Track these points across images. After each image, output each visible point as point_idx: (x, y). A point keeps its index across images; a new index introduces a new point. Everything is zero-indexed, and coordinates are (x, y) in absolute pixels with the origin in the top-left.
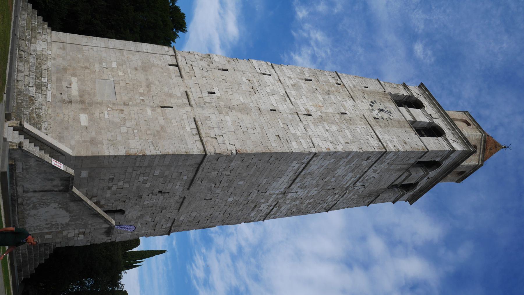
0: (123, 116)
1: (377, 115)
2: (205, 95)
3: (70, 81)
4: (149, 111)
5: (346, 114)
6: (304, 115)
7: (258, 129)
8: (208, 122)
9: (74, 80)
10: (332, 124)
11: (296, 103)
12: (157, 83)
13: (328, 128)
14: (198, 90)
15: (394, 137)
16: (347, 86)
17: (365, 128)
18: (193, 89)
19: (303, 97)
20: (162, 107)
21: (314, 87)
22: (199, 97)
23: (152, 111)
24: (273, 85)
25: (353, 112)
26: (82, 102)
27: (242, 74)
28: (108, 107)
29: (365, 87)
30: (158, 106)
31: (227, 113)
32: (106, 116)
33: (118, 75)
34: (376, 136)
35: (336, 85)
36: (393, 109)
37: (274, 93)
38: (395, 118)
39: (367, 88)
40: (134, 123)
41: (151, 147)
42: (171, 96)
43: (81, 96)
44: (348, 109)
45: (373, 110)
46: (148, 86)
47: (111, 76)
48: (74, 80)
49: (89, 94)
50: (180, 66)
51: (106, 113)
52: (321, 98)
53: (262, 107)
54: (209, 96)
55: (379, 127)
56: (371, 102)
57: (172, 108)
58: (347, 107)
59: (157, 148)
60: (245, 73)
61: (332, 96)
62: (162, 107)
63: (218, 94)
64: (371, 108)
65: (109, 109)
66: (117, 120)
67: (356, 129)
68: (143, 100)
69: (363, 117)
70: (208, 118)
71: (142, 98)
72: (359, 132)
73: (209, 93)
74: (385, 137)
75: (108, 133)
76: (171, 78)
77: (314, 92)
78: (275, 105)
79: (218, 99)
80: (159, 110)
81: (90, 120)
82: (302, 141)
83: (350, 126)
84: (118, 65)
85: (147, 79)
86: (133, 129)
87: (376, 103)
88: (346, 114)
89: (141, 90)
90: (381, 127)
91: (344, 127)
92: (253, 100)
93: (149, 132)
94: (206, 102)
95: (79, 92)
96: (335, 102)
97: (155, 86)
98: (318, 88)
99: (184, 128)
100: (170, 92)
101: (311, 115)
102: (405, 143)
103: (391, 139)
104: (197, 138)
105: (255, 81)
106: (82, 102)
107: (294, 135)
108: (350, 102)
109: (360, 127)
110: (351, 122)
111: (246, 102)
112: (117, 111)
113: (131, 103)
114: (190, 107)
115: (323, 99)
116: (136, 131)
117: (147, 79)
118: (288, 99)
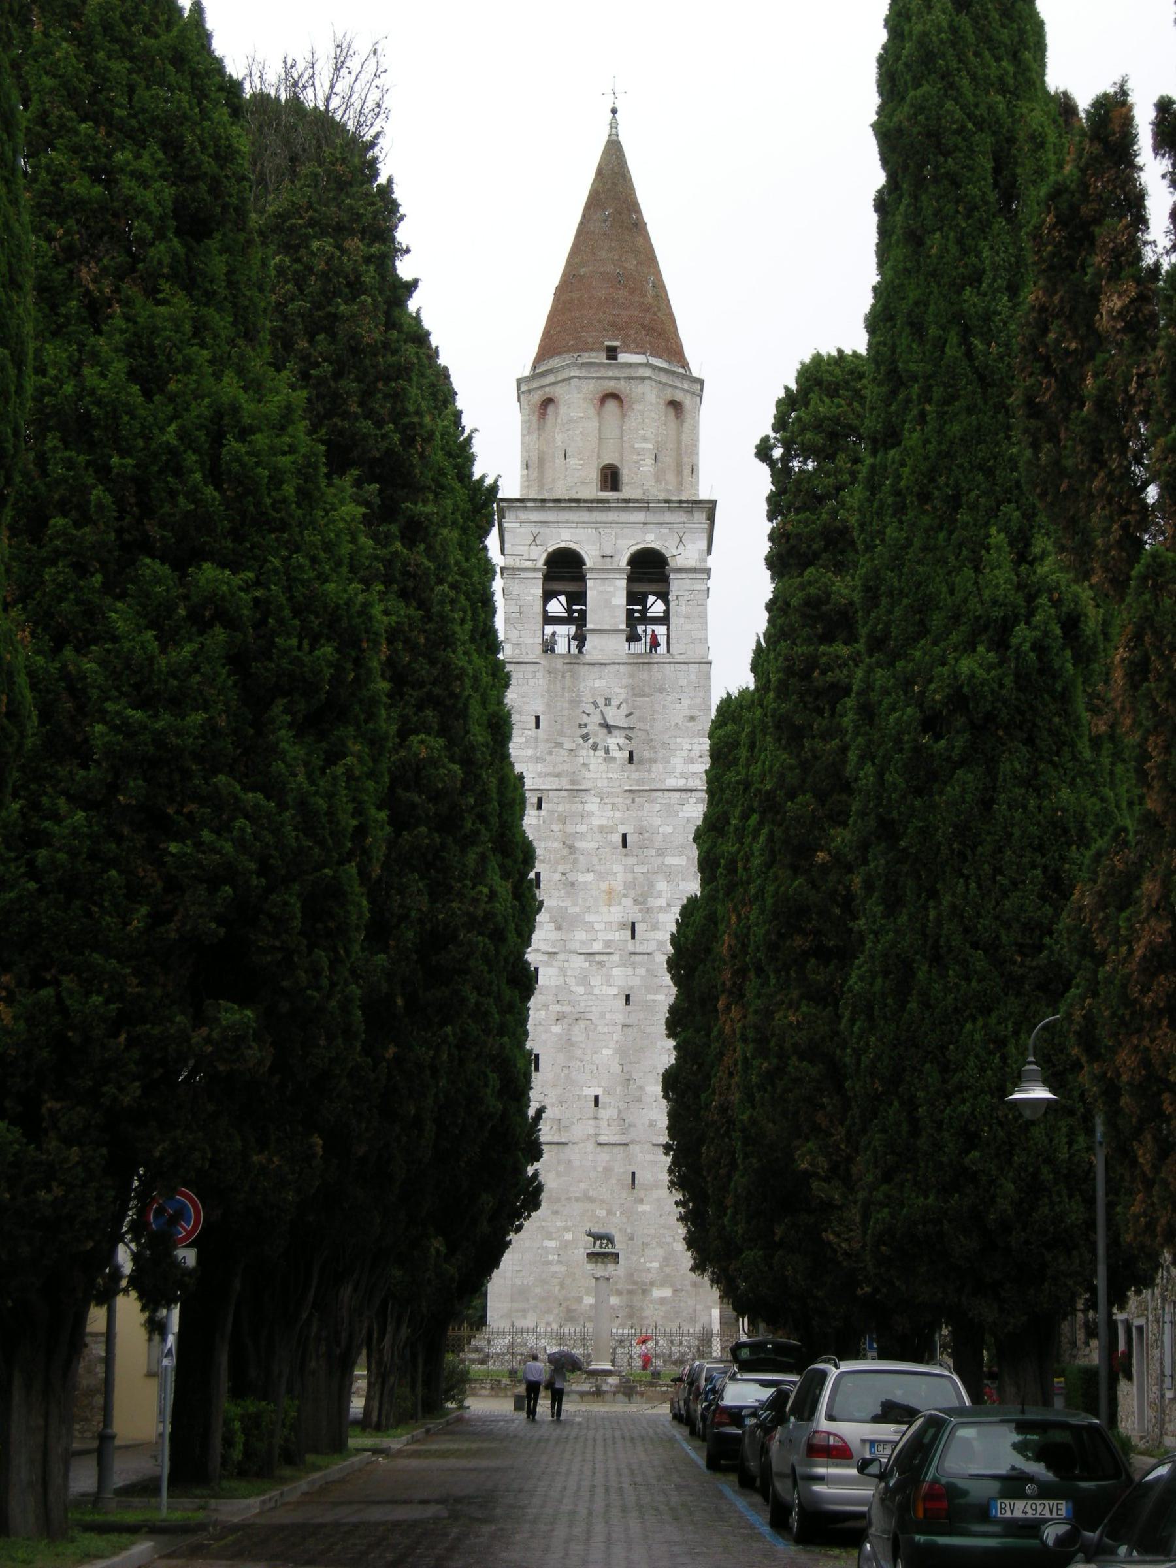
1: (620, 748)
2: (602, 1112)
4: (641, 1208)
5: (624, 836)
6: (633, 937)
10: (652, 886)
11: (608, 943)
12: (583, 1186)
13: (662, 902)
14: (591, 1122)
15: (679, 740)
16: (541, 780)
17: (658, 807)
18: (592, 1132)
19: (589, 918)
20: (633, 1188)
21: (557, 876)
24: (563, 971)
25: (618, 814)
26: (630, 1292)
27: (541, 1028)
29: (537, 727)
34: (677, 795)
35: (543, 813)
36: (597, 683)
37: (584, 980)
38: (623, 696)
39: (537, 718)
40: (666, 1232)
42: (608, 1170)
44: (611, 823)
45: (607, 750)
46: (591, 1200)
47: (576, 1251)
51: (648, 1265)
52: (589, 877)
53: (620, 1018)
54: (604, 1108)
55: (655, 767)
56: (585, 737)
58: (604, 822)
61: (578, 845)
63: (599, 1092)
64: (601, 753)
66: (660, 1252)
67: (664, 835)
69: (632, 795)
71: (618, 1214)
72: (669, 829)
74: (679, 769)
77: (573, 884)
78: (614, 991)
81: (662, 1285)
83: (656, 845)
84: (549, 1236)
85: (577, 1200)
87: (585, 725)
88: (624, 836)
89: (602, 1213)
90: (653, 761)
91: (660, 859)
92: (606, 1030)
96: (595, 845)
98: (561, 868)
100: (600, 1169)
101: (633, 924)
102: (692, 718)
103: (685, 753)
105: (558, 1008)
108: (592, 805)
109: (658, 821)
110: (647, 835)
111: (612, 1044)
113: (629, 1231)
114: (631, 1146)
115: (588, 871)
117: (577, 1200)
118: (598, 958)
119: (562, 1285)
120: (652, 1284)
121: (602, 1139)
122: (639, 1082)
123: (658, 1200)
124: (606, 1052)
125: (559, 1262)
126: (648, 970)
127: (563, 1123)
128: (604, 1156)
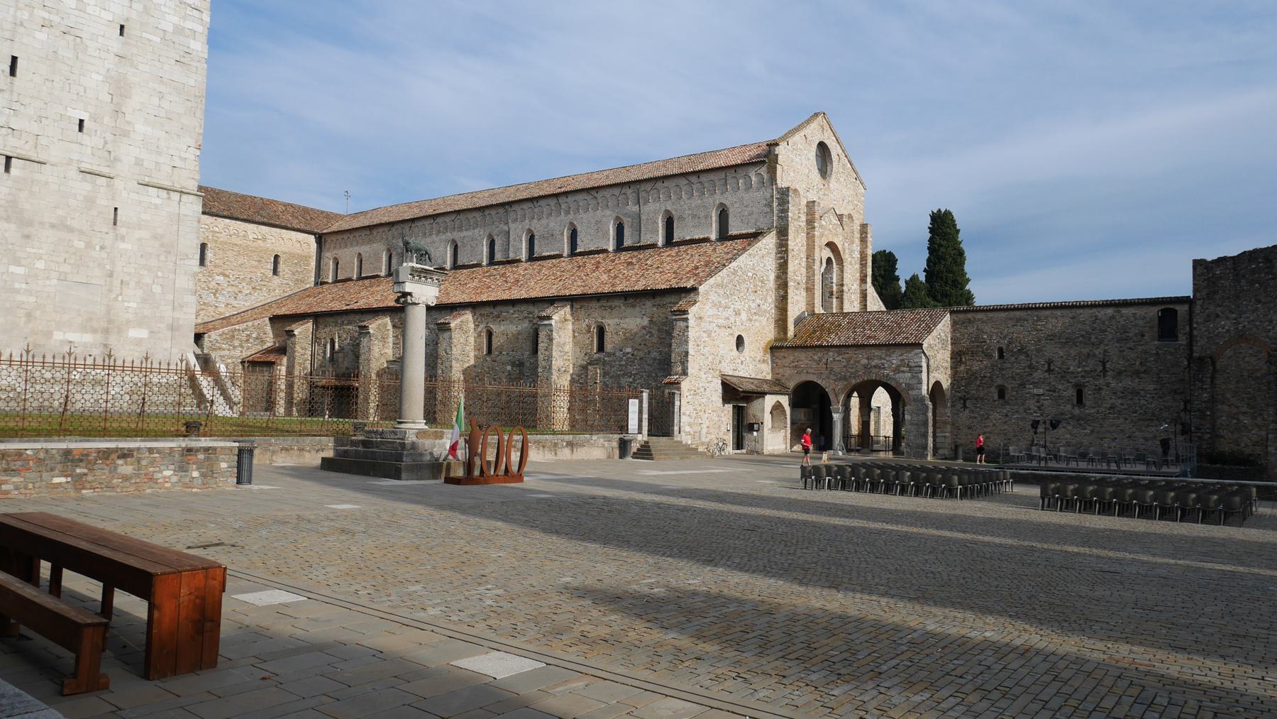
0: (132, 284)
3: (61, 341)
4: (122, 246)
7: (163, 89)
8: (145, 164)
9: (58, 336)
20: (115, 223)
22: (93, 154)
23: (124, 241)
27: (21, 30)
28: (116, 299)
30: (115, 229)
31: (129, 123)
32: (133, 305)
33: (45, 270)
40: (146, 272)
41: (187, 262)
42: (90, 201)
43: (94, 331)
47: (48, 282)
48: (58, 336)
49: (91, 319)
50: (15, 155)
51: (126, 304)
57: (116, 209)
59: (190, 256)
60: (21, 22)
62: (115, 223)
63: (84, 116)
65: (120, 298)
68: (102, 248)
70: (139, 162)
71: (98, 248)
73: (81, 129)
75: (161, 308)
76: (47, 183)
78: (107, 16)
79: (95, 121)
80: (122, 230)
82: (189, 25)
85: (53, 226)
86: (157, 277)
89: (81, 245)
92: (97, 54)
93: (162, 258)
94: (104, 147)
95: (87, 332)
97: (69, 219)
99: (156, 206)
104: (175, 196)
105: (46, 15)
106: (106, 331)
107: (179, 30)
112: (124, 289)
113: (108, 267)
116: (160, 274)
117: (53, 226)
119: (29, 316)
120: (128, 322)
121: (85, 166)
122: (128, 118)
123: (140, 240)
124: (95, 76)
125: (29, 293)
126: (145, 7)
127: (43, 141)
128: (83, 187)
